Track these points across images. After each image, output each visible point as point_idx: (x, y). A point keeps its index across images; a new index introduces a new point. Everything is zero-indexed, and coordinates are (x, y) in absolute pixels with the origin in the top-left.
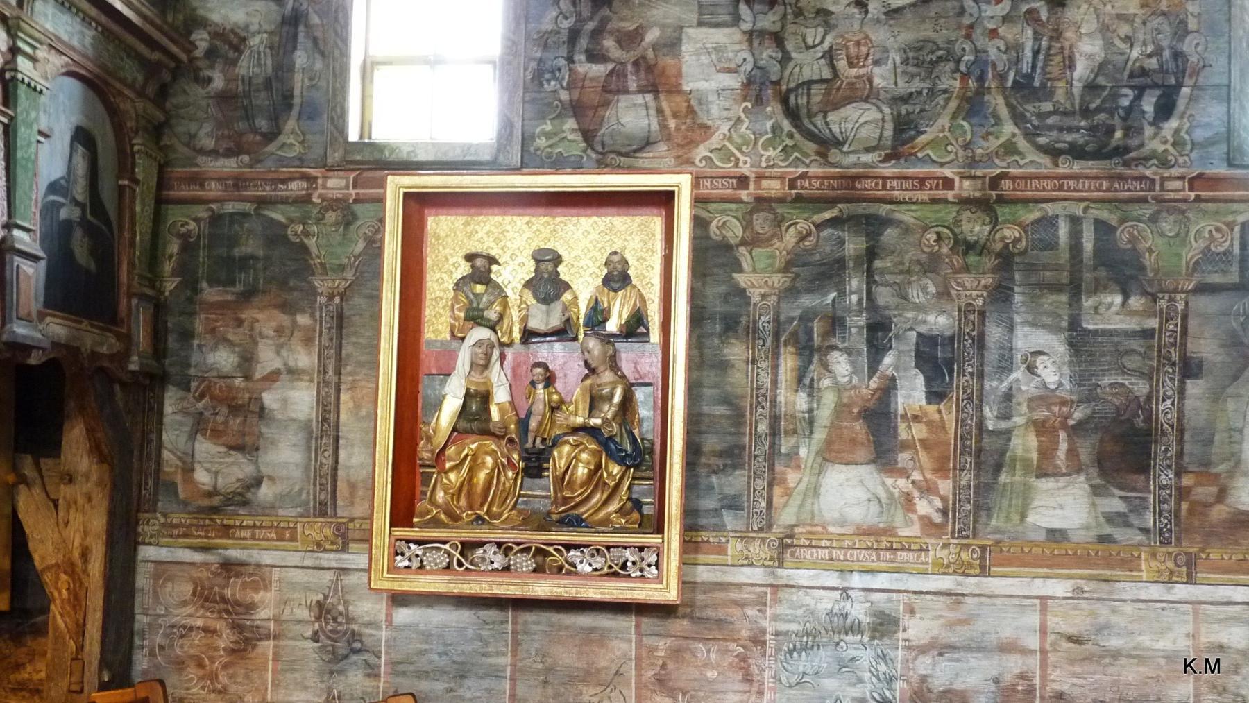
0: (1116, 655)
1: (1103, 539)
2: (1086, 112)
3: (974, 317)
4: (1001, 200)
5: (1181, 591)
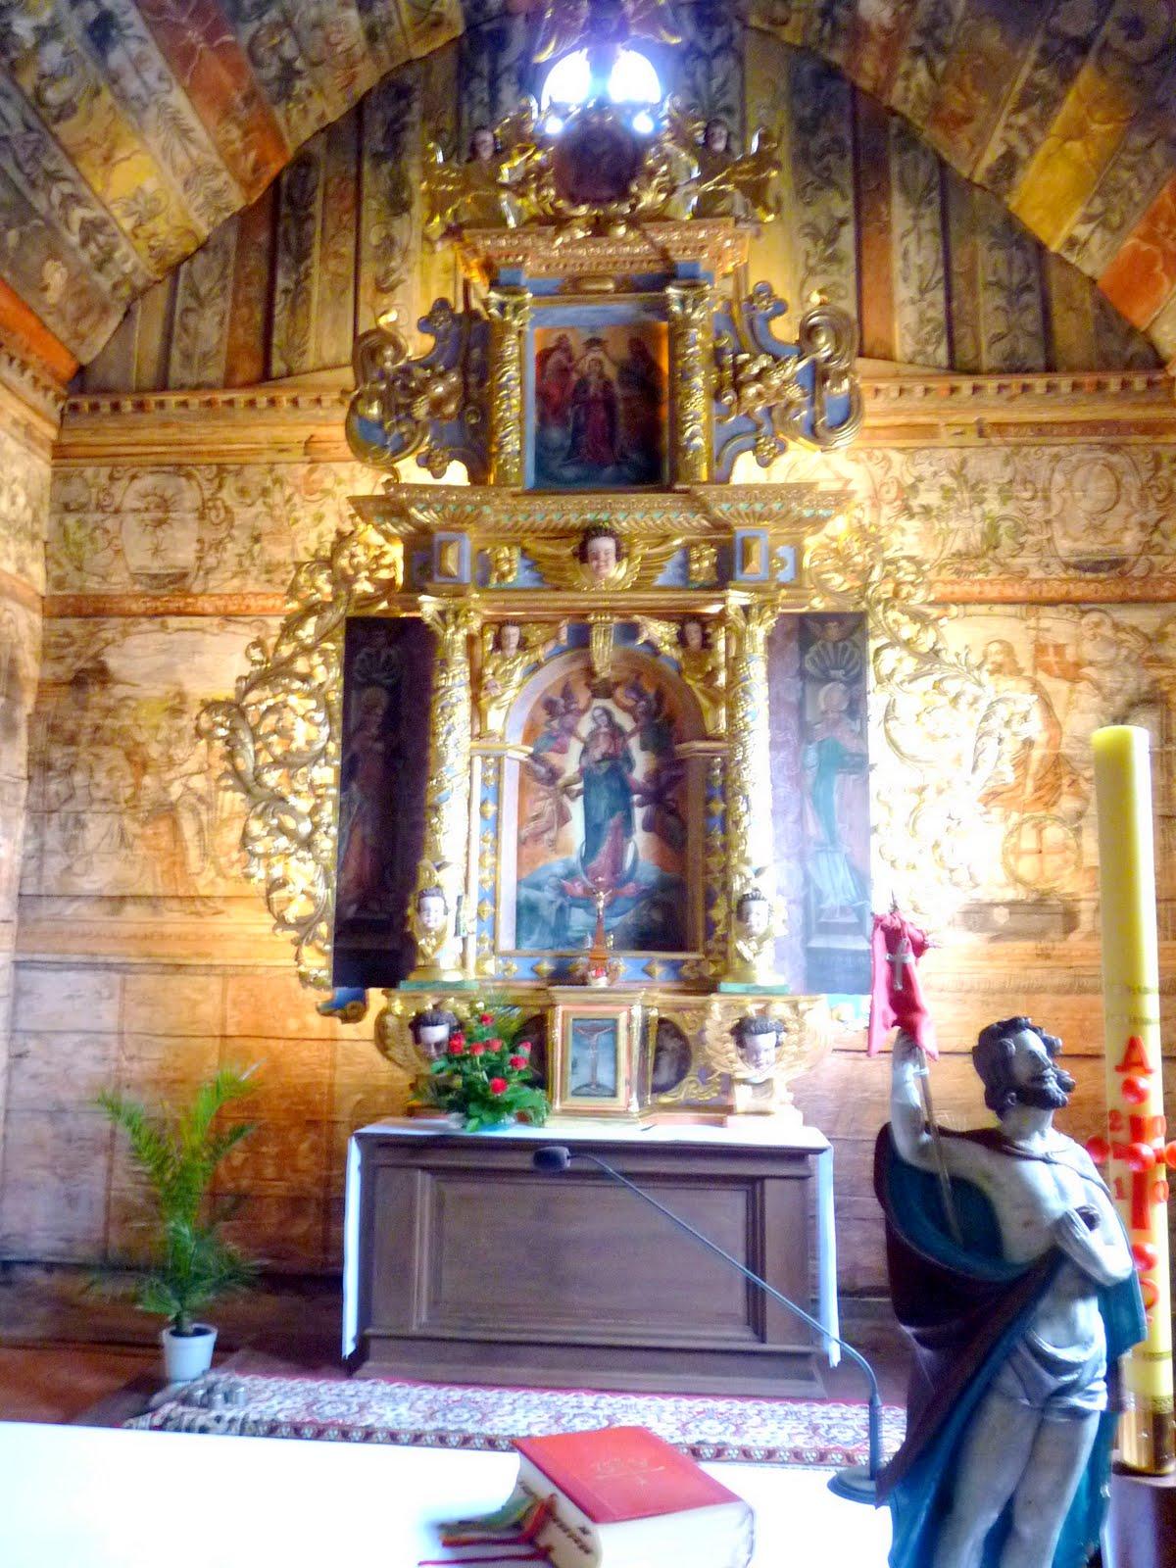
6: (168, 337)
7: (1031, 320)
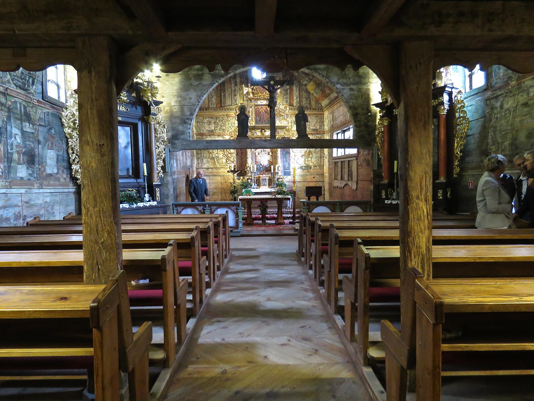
0: (33, 205)
1: (29, 179)
2: (22, 79)
3: (5, 123)
4: (7, 94)
5: (41, 191)
6: (209, 101)
7: (308, 102)
